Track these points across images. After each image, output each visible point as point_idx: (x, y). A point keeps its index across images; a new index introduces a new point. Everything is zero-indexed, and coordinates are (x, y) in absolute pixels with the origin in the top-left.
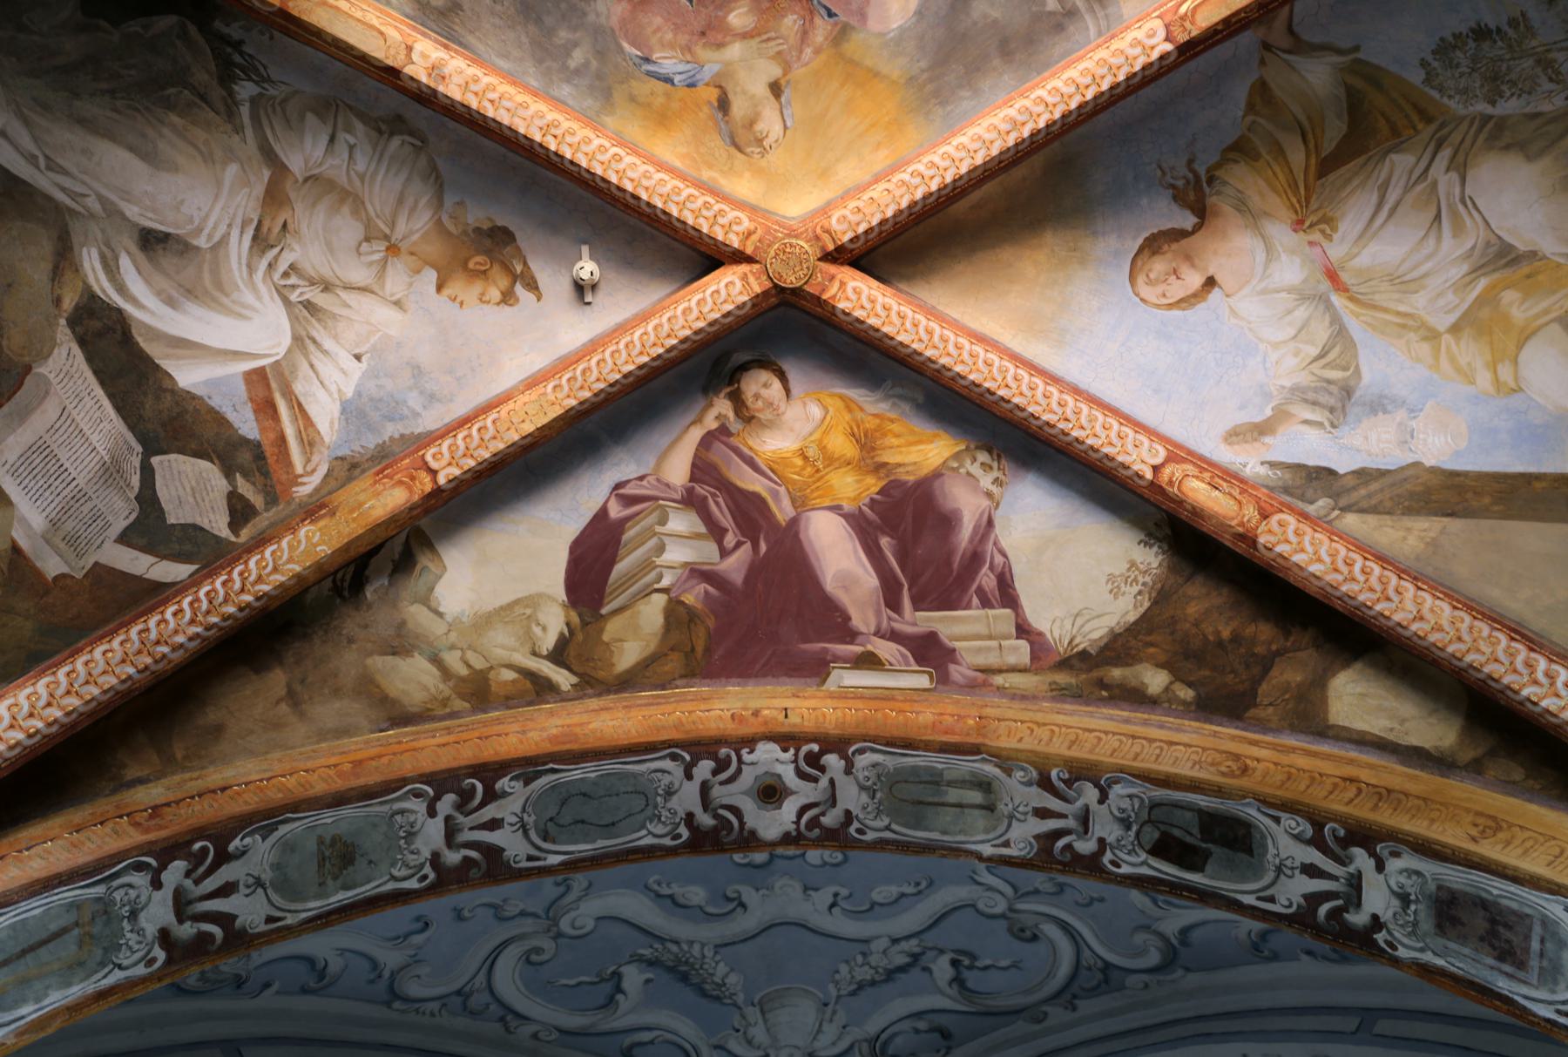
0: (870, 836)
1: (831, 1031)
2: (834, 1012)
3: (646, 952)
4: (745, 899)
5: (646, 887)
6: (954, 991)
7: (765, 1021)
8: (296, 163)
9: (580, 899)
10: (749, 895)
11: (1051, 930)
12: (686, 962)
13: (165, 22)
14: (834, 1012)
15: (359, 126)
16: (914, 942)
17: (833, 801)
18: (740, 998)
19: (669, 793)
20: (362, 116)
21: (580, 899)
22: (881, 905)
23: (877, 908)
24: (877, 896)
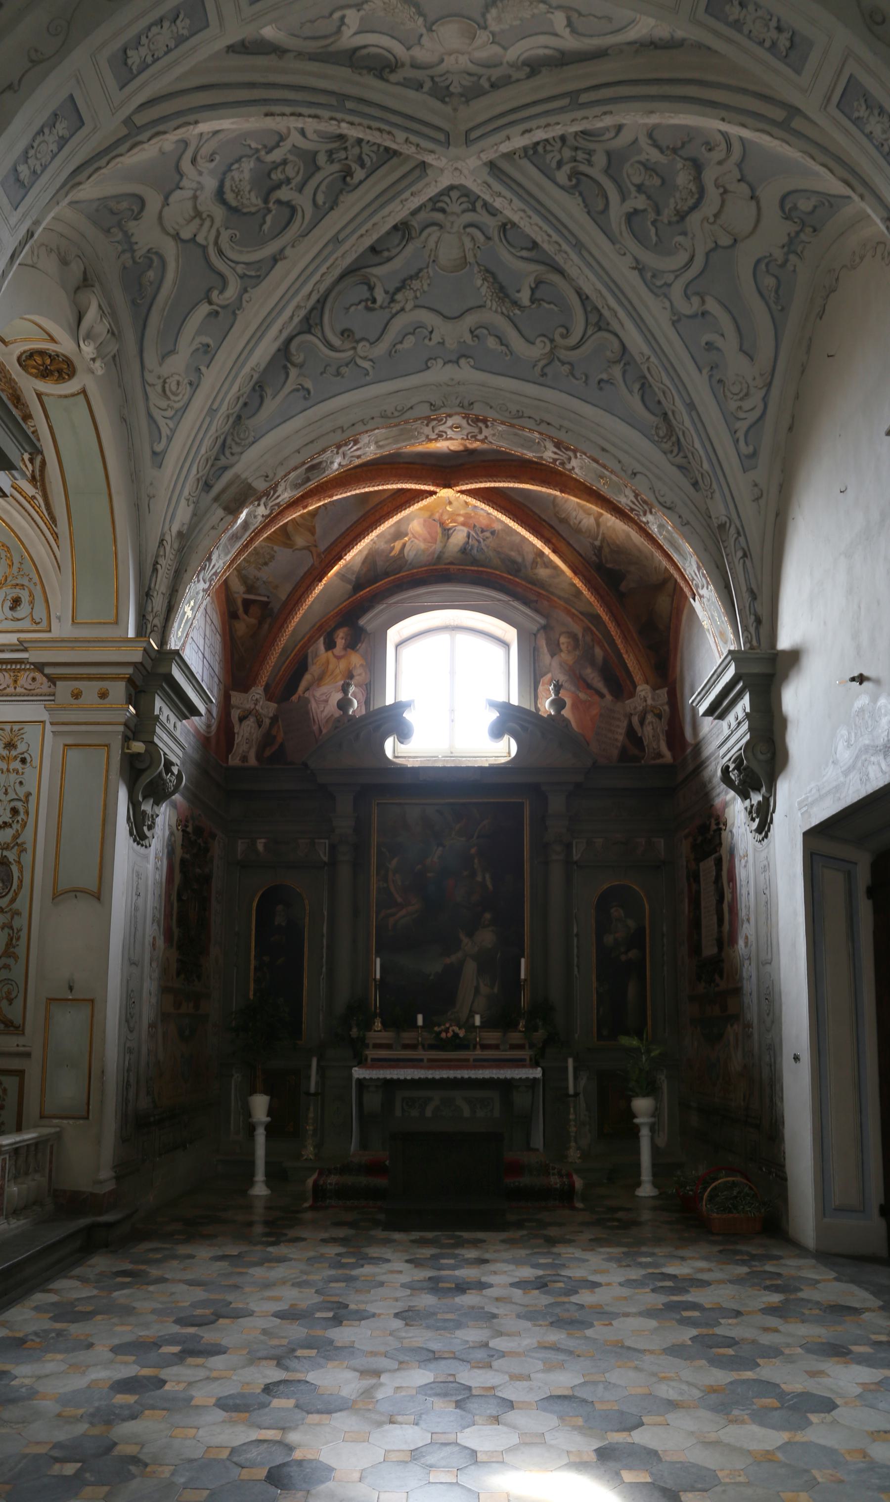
0: (419, 422)
1: (431, 244)
2: (430, 256)
3: (517, 312)
4: (470, 336)
5: (511, 354)
6: (373, 280)
7: (464, 251)
8: (592, 520)
9: (539, 360)
10: (468, 337)
11: (336, 342)
12: (499, 298)
13: (609, 566)
14: (430, 256)
15: (572, 523)
16: (394, 311)
17: (433, 428)
18: (476, 269)
19: (494, 435)
20: (569, 525)
21: (539, 360)
22: (410, 333)
23: (412, 331)
24: (411, 338)
